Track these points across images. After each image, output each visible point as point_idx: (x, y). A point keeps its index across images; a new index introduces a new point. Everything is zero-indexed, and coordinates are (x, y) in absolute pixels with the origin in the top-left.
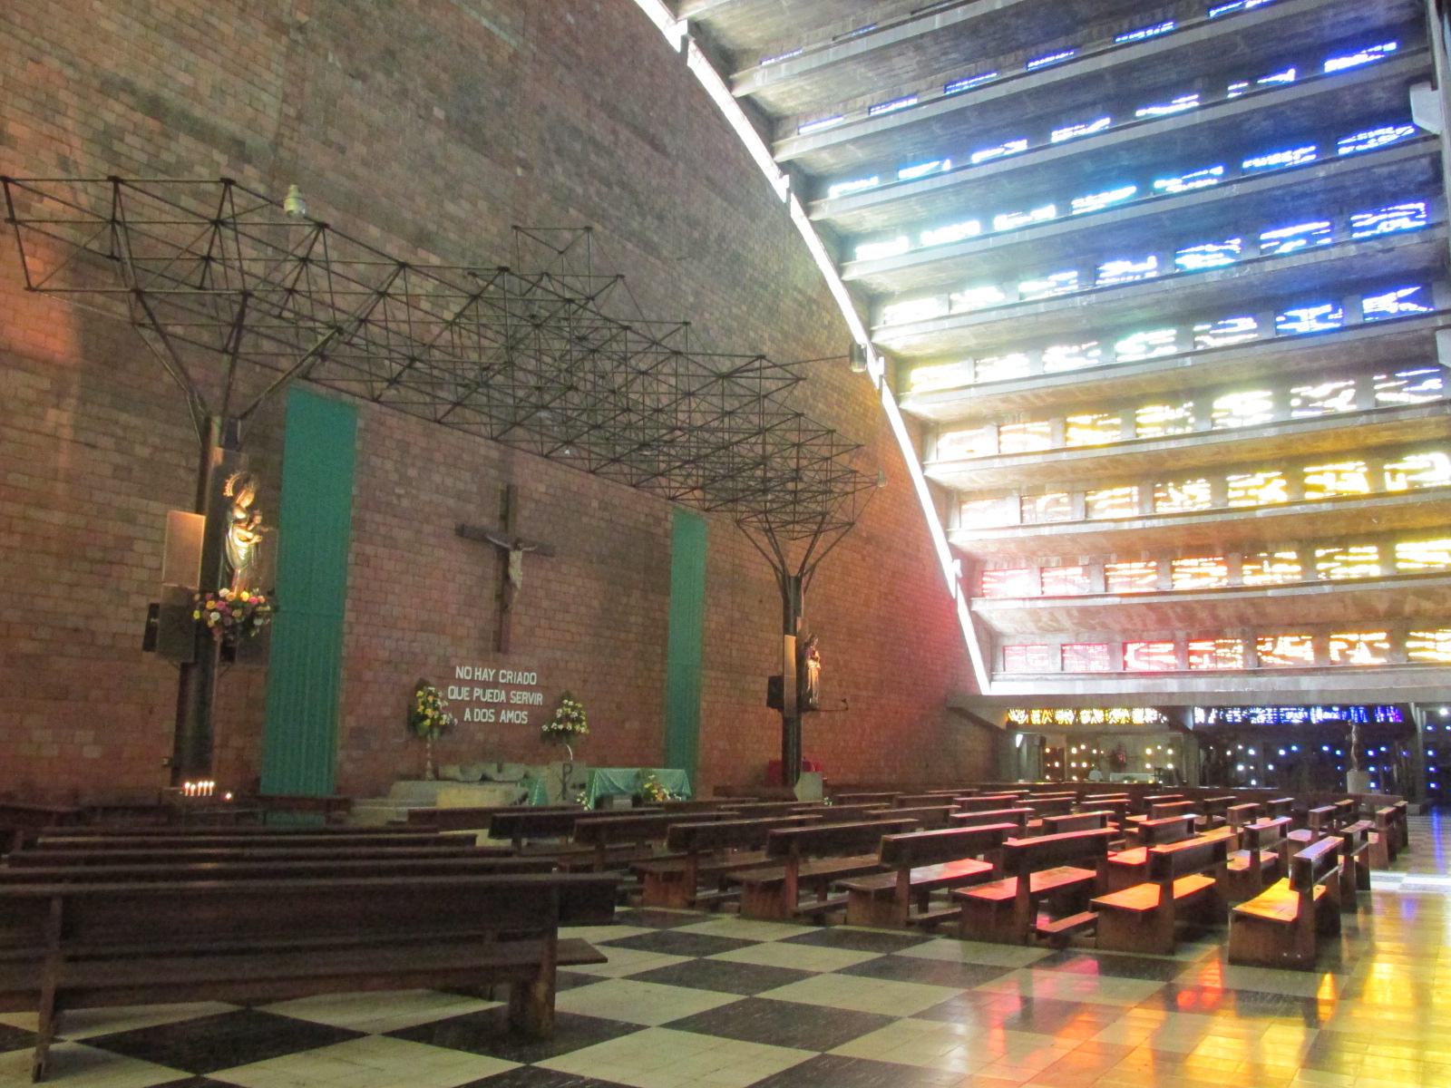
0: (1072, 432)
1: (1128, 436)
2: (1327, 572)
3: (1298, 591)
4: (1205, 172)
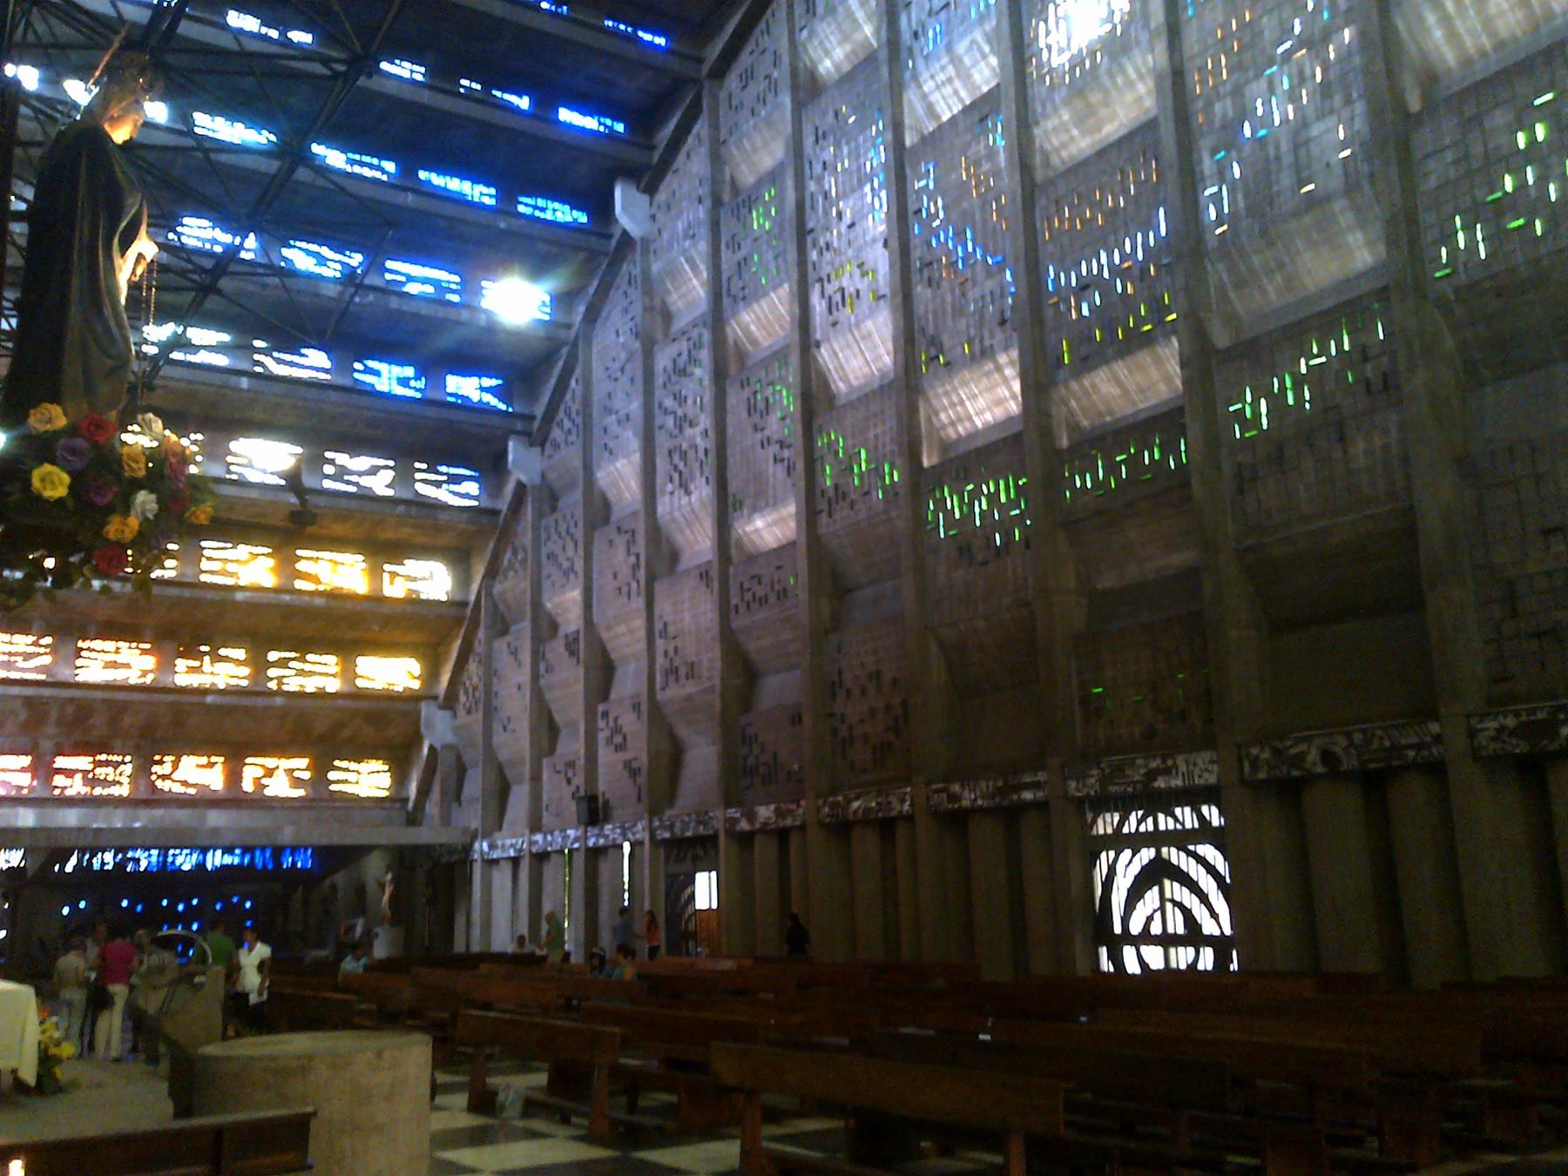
2: (280, 679)
3: (245, 701)
4: (375, 161)
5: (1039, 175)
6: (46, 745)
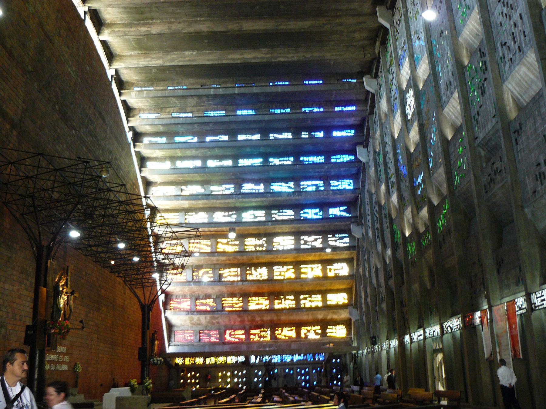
0: (219, 245)
1: (242, 249)
4: (287, 159)
6: (247, 327)
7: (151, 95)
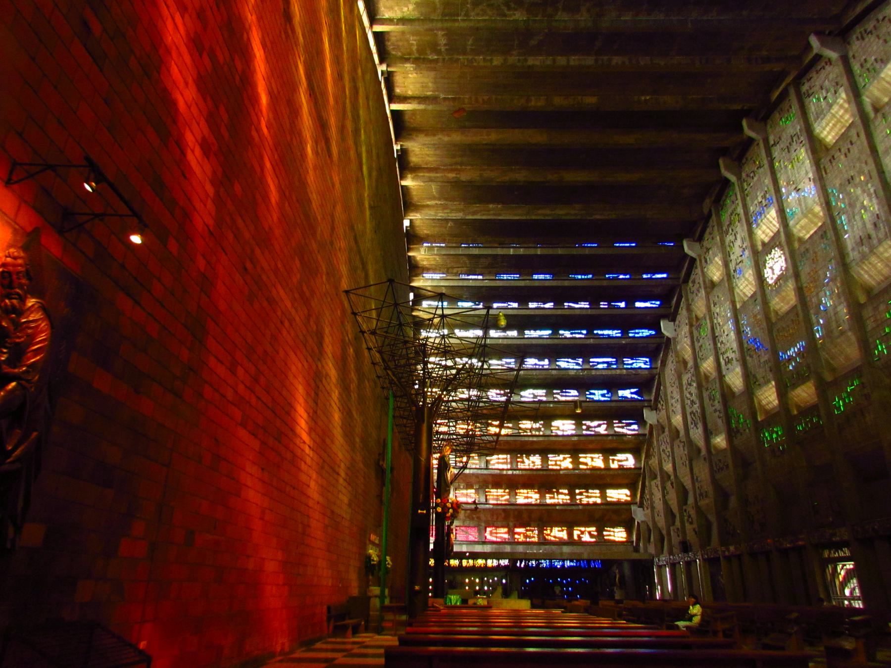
2: (580, 499)
4: (579, 331)
5: (774, 320)
6: (511, 524)
7: (444, 252)
